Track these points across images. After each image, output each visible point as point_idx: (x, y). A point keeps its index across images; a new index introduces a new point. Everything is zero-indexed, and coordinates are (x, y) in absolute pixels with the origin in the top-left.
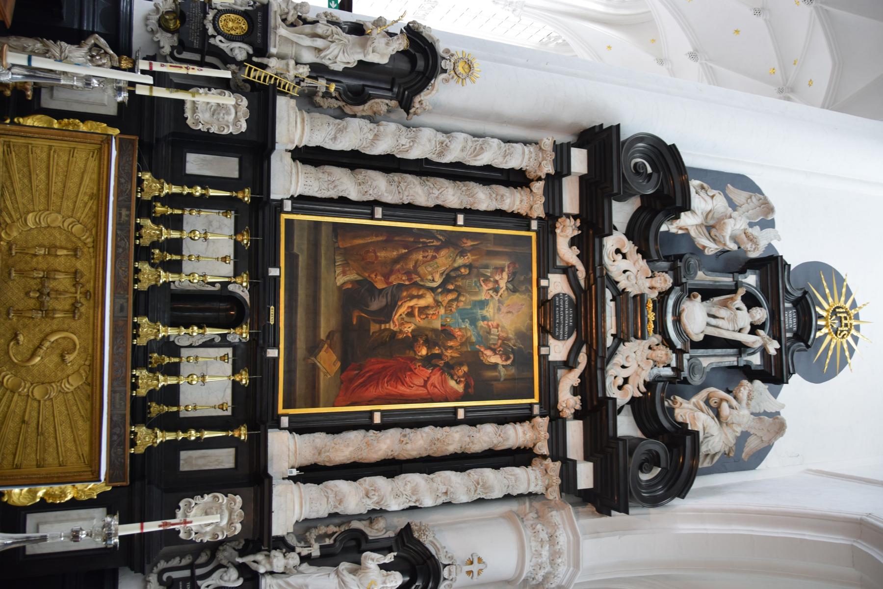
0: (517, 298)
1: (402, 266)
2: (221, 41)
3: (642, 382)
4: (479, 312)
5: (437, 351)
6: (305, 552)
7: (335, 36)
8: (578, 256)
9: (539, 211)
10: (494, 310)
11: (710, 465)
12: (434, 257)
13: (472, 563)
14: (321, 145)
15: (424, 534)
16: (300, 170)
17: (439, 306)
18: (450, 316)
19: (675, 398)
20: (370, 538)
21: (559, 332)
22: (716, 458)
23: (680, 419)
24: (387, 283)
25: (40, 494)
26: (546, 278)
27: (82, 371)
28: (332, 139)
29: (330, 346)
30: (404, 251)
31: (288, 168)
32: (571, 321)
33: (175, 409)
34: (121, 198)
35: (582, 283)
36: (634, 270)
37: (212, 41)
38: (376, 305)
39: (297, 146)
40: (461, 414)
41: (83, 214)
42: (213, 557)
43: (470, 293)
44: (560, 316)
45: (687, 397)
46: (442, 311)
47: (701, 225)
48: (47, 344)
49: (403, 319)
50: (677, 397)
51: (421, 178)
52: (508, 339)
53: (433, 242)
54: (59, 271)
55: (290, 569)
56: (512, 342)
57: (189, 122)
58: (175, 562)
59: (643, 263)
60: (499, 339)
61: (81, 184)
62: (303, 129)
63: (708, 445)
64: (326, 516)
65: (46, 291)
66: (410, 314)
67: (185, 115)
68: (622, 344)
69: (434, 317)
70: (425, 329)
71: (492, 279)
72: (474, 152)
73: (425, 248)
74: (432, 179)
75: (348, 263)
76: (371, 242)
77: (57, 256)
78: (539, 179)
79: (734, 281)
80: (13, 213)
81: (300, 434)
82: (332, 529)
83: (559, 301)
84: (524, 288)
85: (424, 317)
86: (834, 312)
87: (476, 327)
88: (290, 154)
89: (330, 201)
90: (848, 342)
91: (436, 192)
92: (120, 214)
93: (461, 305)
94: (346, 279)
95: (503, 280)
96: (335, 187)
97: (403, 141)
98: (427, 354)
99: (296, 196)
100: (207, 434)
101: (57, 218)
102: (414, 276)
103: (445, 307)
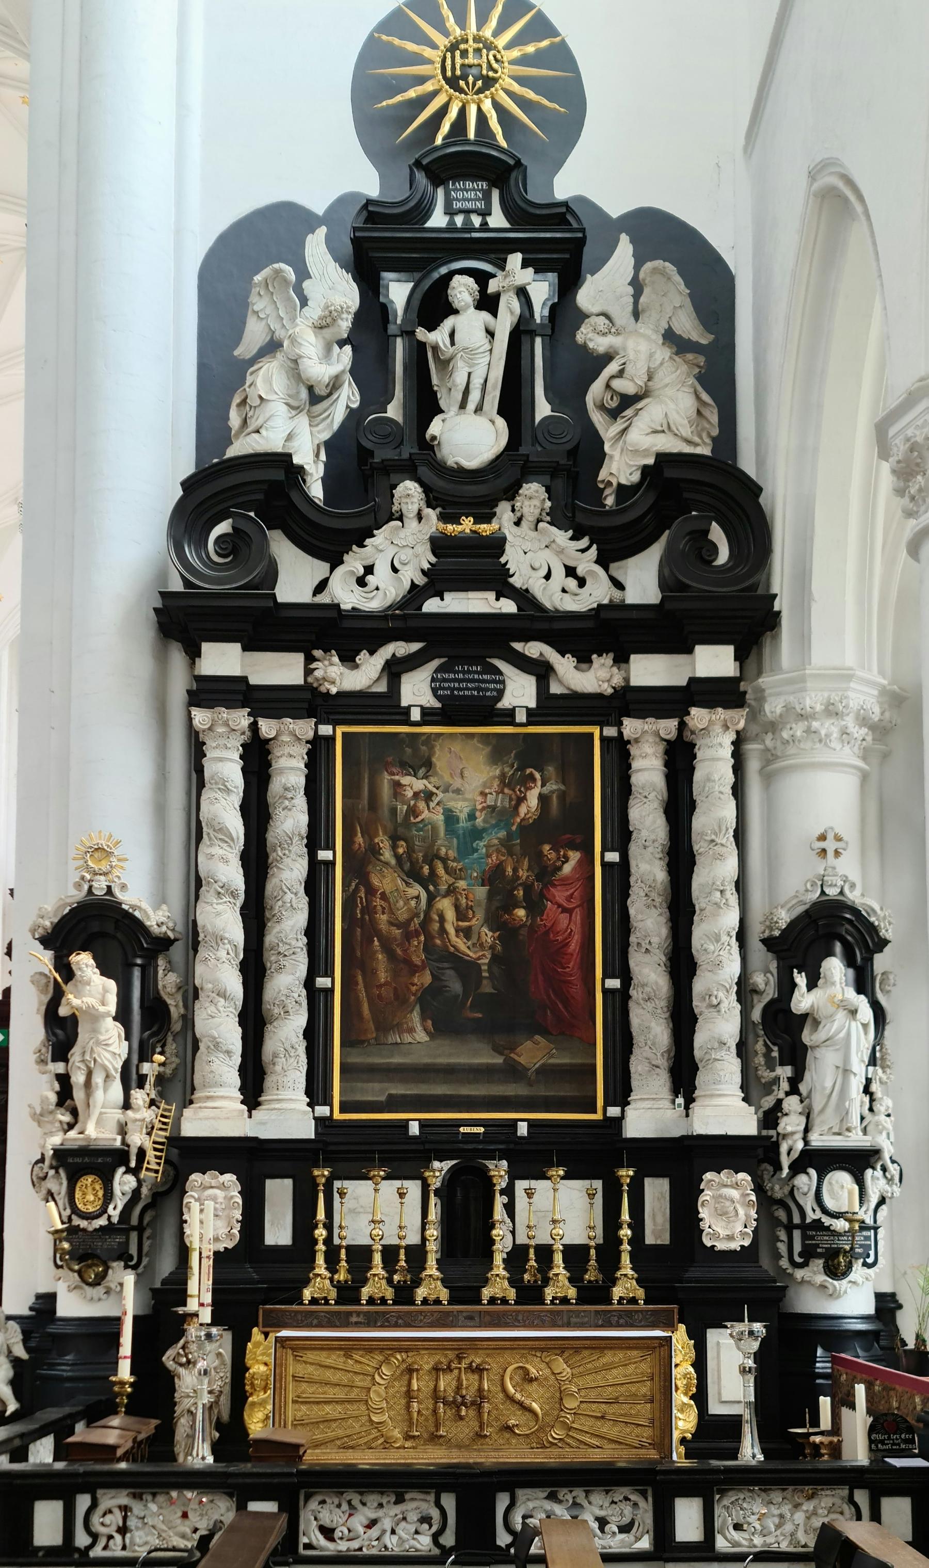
0: (440, 760)
1: (398, 945)
2: (115, 1208)
3: (574, 543)
4: (463, 824)
5: (520, 893)
6: (785, 1086)
7: (87, 1057)
8: (372, 653)
9: (305, 728)
10: (459, 800)
11: (716, 411)
12: (384, 896)
13: (824, 851)
14: (237, 1068)
15: (777, 922)
16: (275, 1097)
17: (455, 889)
18: (469, 871)
19: (603, 481)
20: (776, 996)
21: (492, 690)
22: (705, 397)
23: (636, 477)
24: (423, 967)
25: (686, 1400)
26: (407, 710)
27: (548, 1360)
28: (230, 1057)
29: (513, 1050)
30: (376, 943)
31: (273, 1115)
32: (474, 668)
33: (593, 1252)
34: (338, 1324)
35: (415, 647)
36: (391, 552)
37: (115, 1220)
38: (456, 986)
39: (242, 1102)
40: (613, 857)
41: (370, 1362)
42: (781, 1203)
43: (434, 841)
44: (467, 689)
45: (599, 457)
46: (462, 884)
47: (311, 417)
48: (518, 1396)
49: (474, 945)
50: (600, 478)
51: (269, 920)
52: (503, 775)
53: (361, 898)
54: (436, 1386)
55: (804, 1108)
56: (506, 769)
57: (230, 1245)
58: (782, 1248)
59: (380, 537)
60: (502, 792)
61: (334, 1368)
62: (222, 1097)
63: (681, 425)
64: (739, 1060)
65: (459, 1399)
66: (467, 933)
67: (222, 1250)
68: (511, 580)
69: (471, 896)
70: (488, 911)
71: (412, 803)
72: (226, 842)
73: (369, 910)
74: (269, 902)
75: (397, 1024)
76: (366, 991)
77: (418, 1390)
78: (254, 727)
79: (402, 335)
80: (372, 1436)
81: (631, 1091)
82: (760, 1047)
83: (444, 689)
84: (424, 748)
85: (470, 912)
86: (453, 82)
87: (484, 830)
88: (253, 1112)
89: (310, 1052)
90: (508, 47)
91: (289, 896)
92: (356, 1323)
93: (452, 854)
94: (419, 1028)
95: (413, 784)
96: (293, 1047)
97: (222, 954)
98: (524, 907)
99: (308, 1100)
100: (625, 1216)
101: (375, 1391)
102: (412, 928)
103: (456, 879)
